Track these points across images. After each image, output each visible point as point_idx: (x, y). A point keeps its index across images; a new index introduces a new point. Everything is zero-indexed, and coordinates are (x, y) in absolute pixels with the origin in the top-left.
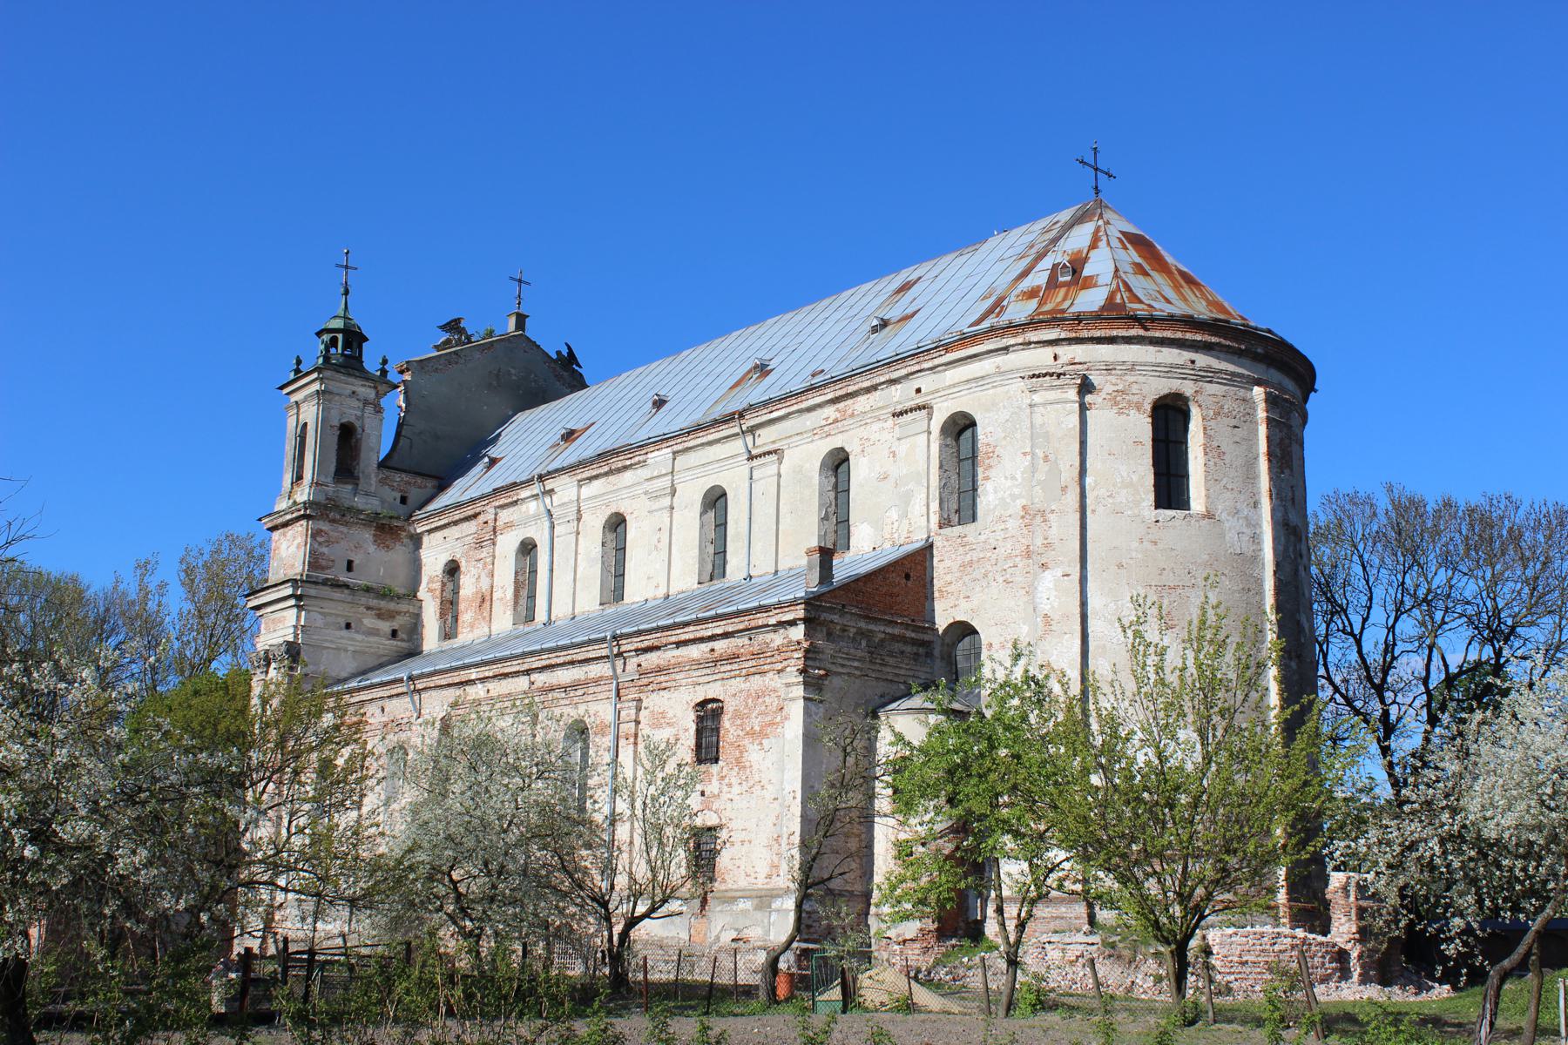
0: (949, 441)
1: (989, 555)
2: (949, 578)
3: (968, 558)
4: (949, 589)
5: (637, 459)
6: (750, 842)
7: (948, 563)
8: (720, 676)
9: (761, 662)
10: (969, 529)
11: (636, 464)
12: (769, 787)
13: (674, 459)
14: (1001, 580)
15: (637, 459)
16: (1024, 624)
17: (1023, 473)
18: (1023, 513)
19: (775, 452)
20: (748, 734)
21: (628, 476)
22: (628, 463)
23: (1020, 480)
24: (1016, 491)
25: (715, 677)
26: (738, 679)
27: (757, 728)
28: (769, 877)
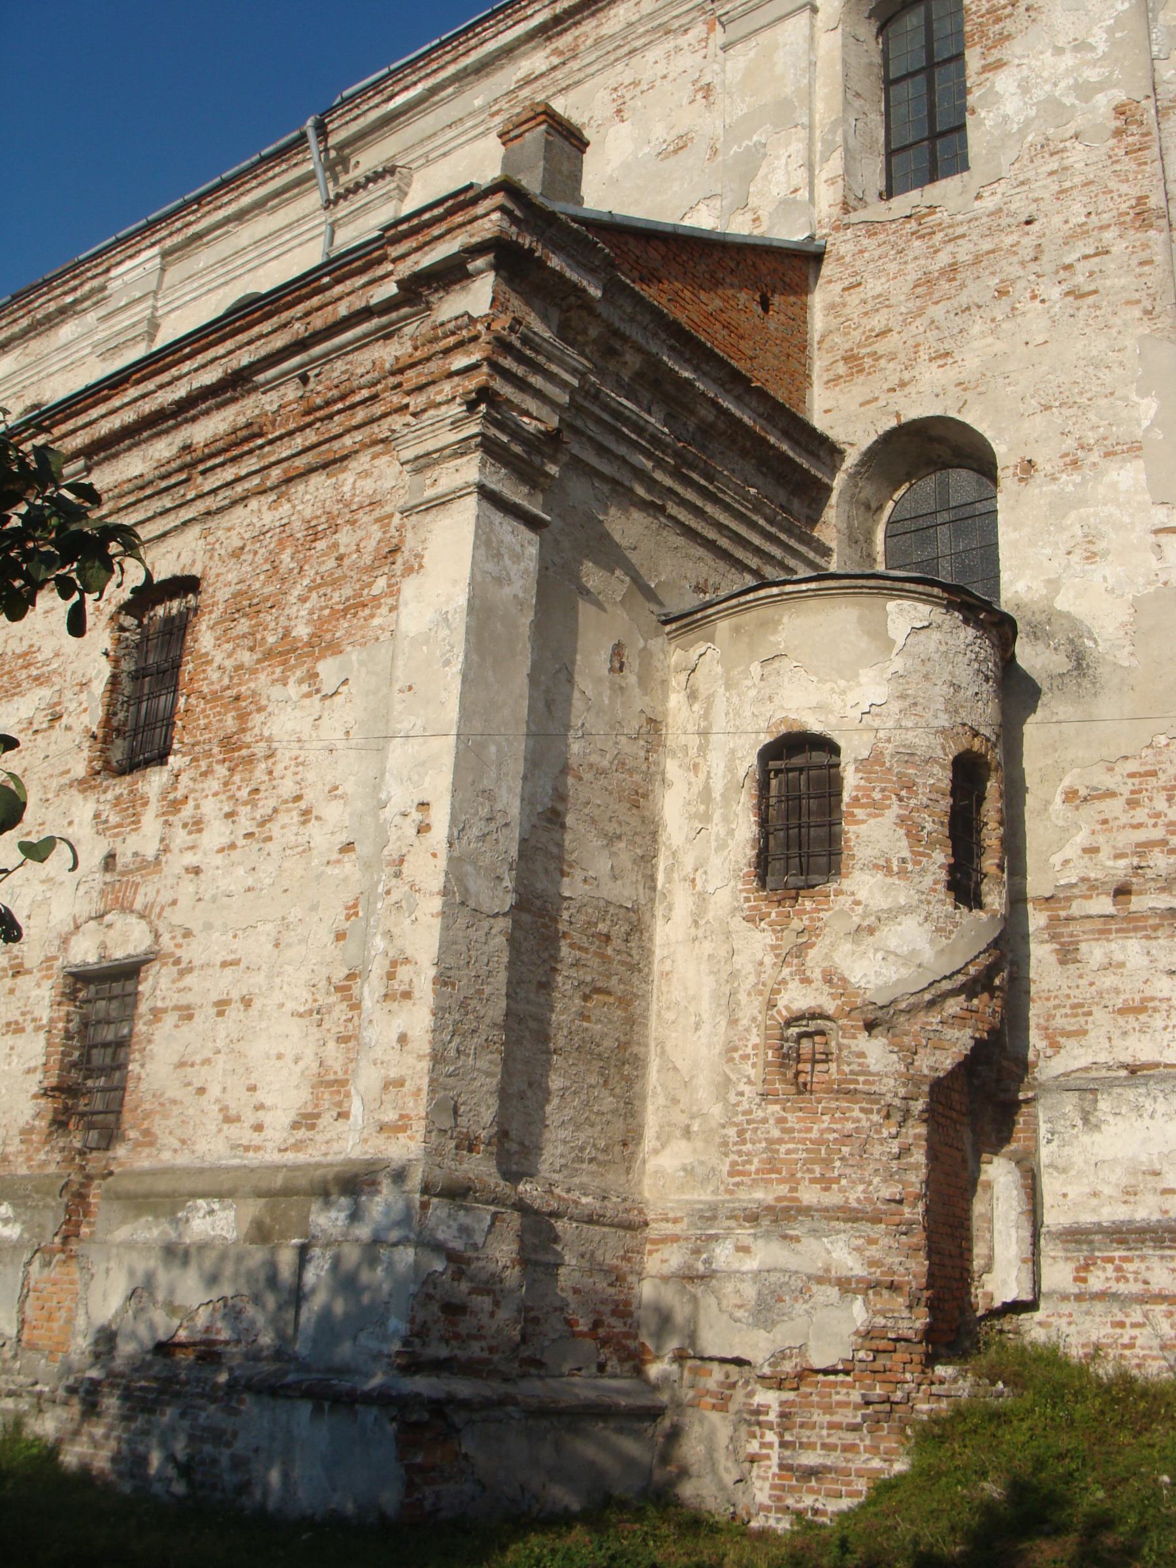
0: (867, 31)
1: (1013, 238)
2: (877, 322)
3: (943, 259)
4: (881, 347)
5: (87, 287)
6: (247, 1002)
7: (874, 287)
8: (201, 506)
9: (335, 427)
10: (946, 190)
11: (85, 298)
12: (332, 812)
13: (163, 270)
14: (1055, 293)
15: (87, 287)
16: (1143, 393)
17: (1110, 31)
18: (1119, 123)
19: (390, 171)
20: (269, 655)
21: (67, 331)
22: (69, 299)
23: (1102, 48)
24: (1092, 75)
25: (186, 514)
26: (253, 504)
27: (302, 631)
28: (307, 1120)
